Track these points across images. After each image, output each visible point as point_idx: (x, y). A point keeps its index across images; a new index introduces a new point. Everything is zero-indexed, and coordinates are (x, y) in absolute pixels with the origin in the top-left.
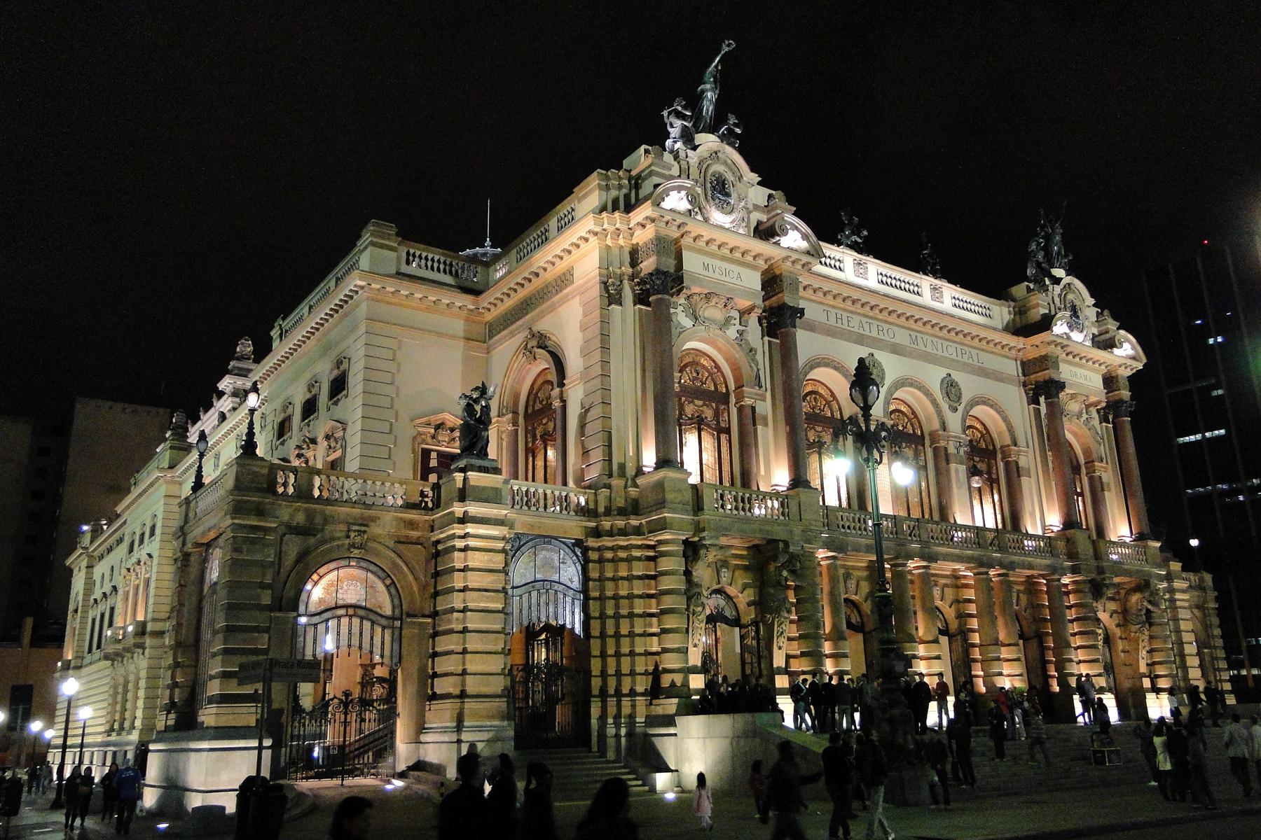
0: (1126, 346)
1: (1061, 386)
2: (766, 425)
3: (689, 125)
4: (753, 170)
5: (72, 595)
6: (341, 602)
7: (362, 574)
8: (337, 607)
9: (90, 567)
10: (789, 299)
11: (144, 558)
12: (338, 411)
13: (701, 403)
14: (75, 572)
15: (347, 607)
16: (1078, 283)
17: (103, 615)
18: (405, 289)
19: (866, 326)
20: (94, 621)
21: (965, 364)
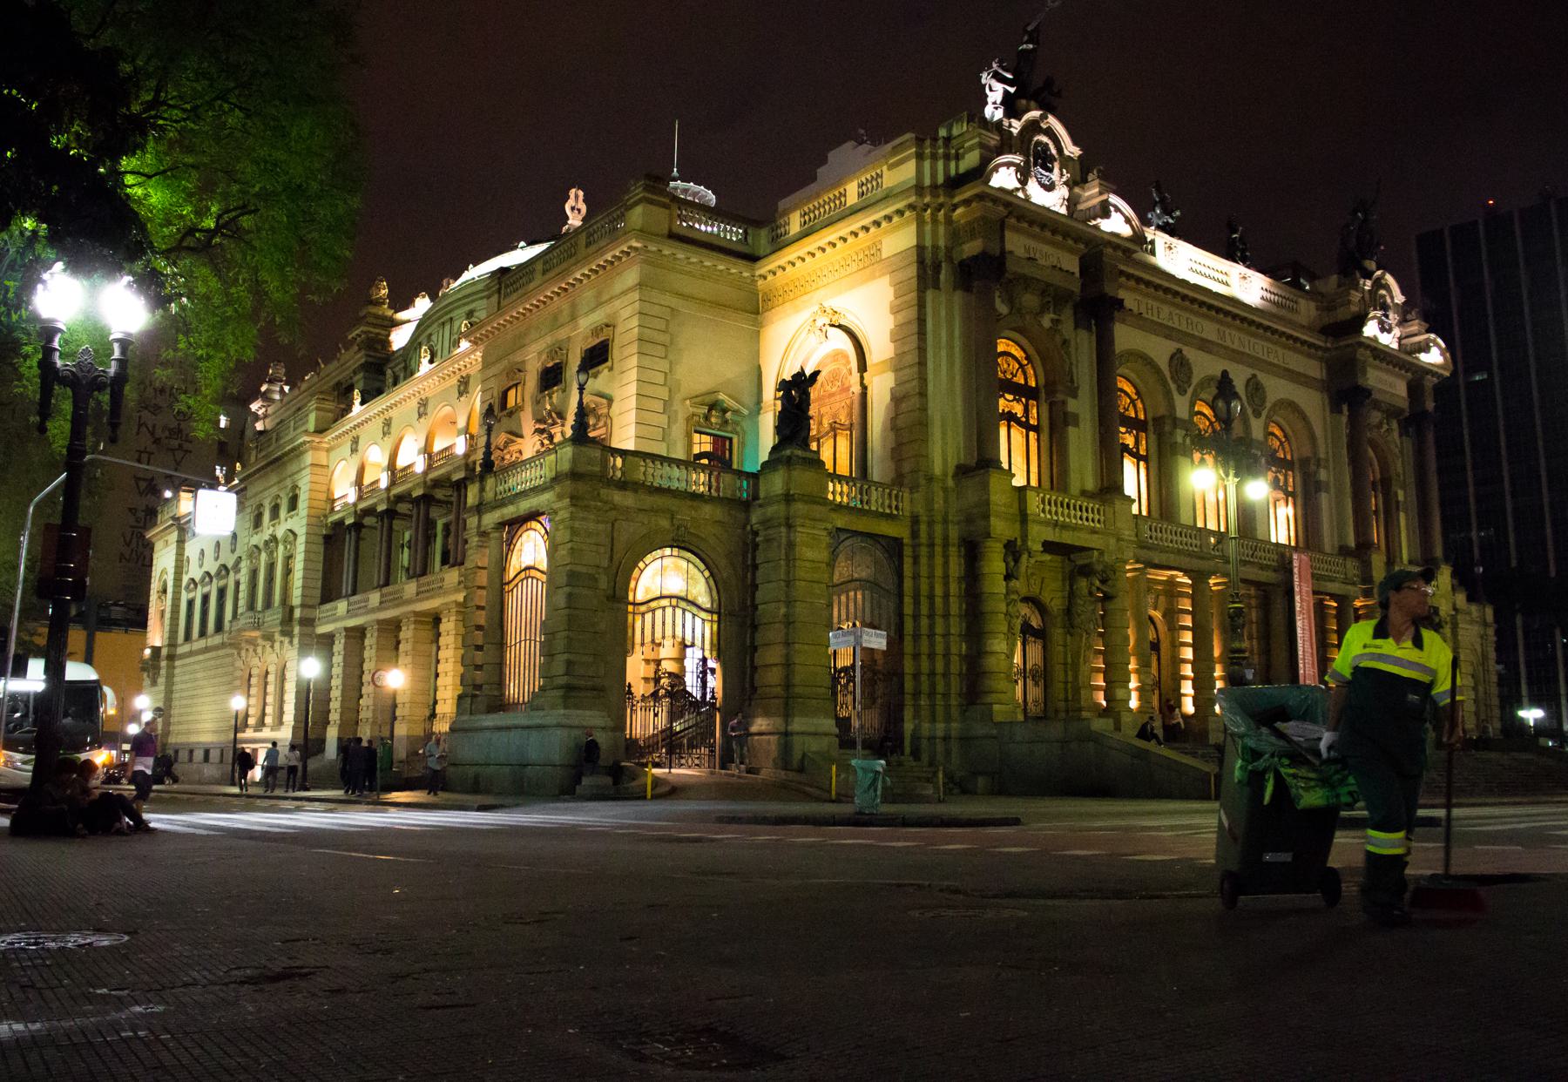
0: (1435, 351)
1: (1367, 393)
2: (1076, 425)
3: (1012, 90)
4: (1075, 143)
5: (156, 573)
6: (665, 593)
7: (684, 564)
8: (662, 597)
9: (181, 542)
10: (1109, 289)
11: (280, 533)
12: (595, 384)
13: (1010, 397)
14: (158, 546)
15: (671, 597)
16: (1389, 279)
17: (206, 598)
18: (681, 253)
19: (1176, 318)
20: (191, 603)
21: (1271, 364)
